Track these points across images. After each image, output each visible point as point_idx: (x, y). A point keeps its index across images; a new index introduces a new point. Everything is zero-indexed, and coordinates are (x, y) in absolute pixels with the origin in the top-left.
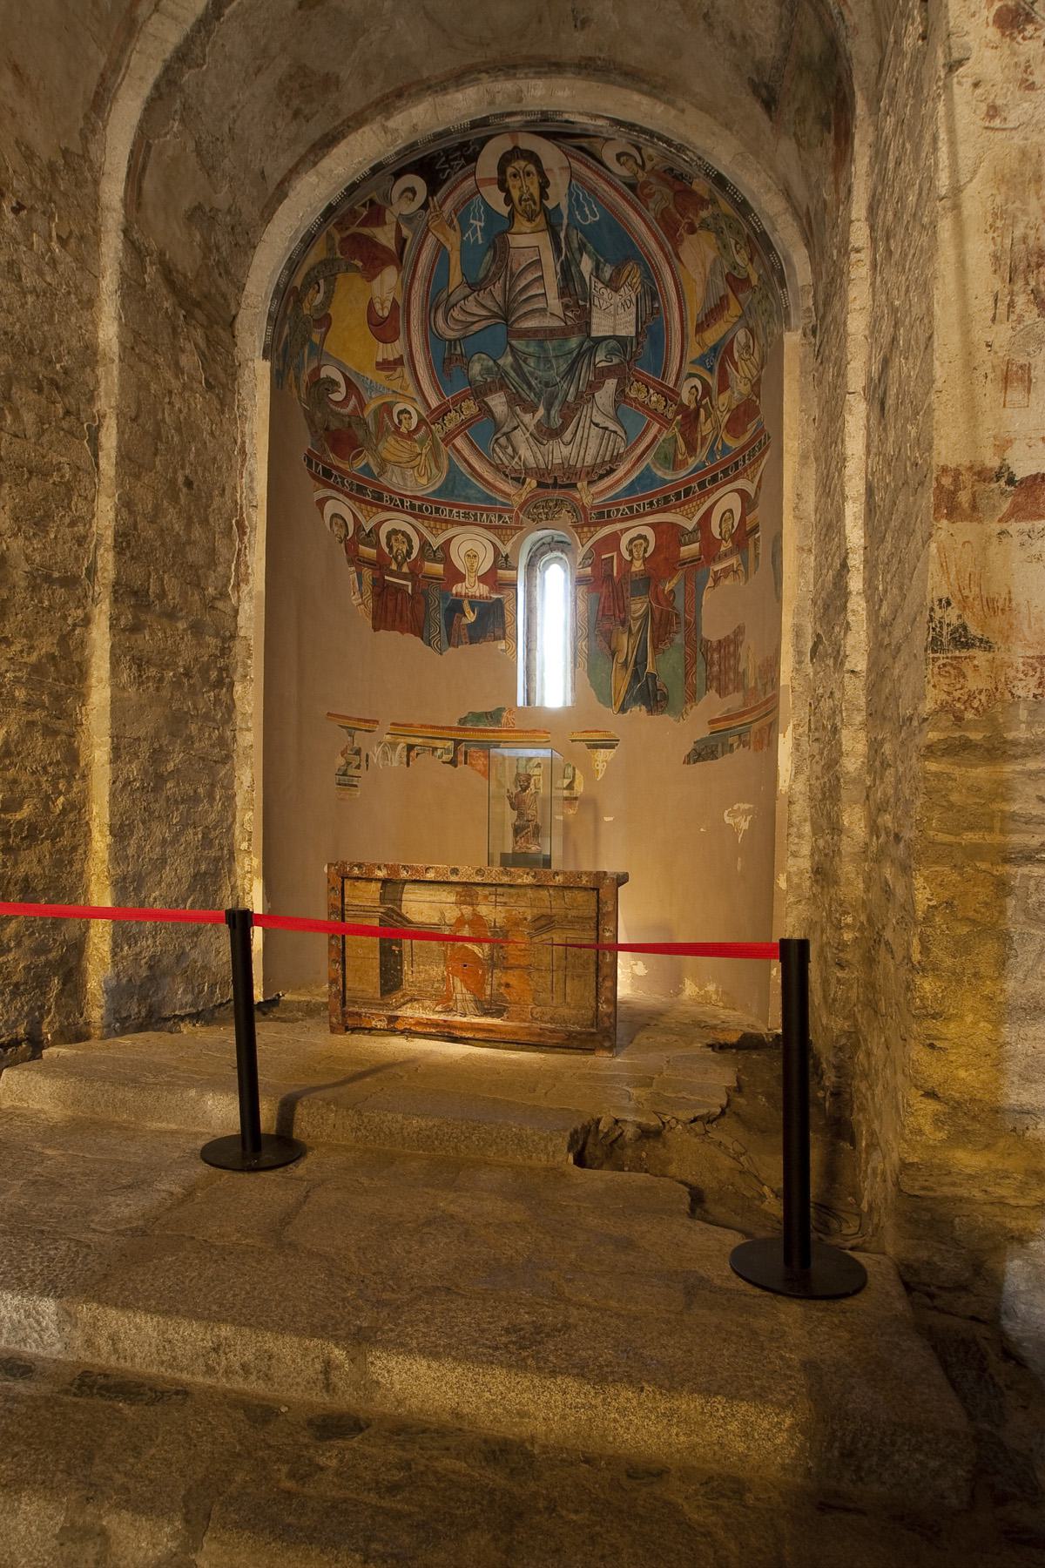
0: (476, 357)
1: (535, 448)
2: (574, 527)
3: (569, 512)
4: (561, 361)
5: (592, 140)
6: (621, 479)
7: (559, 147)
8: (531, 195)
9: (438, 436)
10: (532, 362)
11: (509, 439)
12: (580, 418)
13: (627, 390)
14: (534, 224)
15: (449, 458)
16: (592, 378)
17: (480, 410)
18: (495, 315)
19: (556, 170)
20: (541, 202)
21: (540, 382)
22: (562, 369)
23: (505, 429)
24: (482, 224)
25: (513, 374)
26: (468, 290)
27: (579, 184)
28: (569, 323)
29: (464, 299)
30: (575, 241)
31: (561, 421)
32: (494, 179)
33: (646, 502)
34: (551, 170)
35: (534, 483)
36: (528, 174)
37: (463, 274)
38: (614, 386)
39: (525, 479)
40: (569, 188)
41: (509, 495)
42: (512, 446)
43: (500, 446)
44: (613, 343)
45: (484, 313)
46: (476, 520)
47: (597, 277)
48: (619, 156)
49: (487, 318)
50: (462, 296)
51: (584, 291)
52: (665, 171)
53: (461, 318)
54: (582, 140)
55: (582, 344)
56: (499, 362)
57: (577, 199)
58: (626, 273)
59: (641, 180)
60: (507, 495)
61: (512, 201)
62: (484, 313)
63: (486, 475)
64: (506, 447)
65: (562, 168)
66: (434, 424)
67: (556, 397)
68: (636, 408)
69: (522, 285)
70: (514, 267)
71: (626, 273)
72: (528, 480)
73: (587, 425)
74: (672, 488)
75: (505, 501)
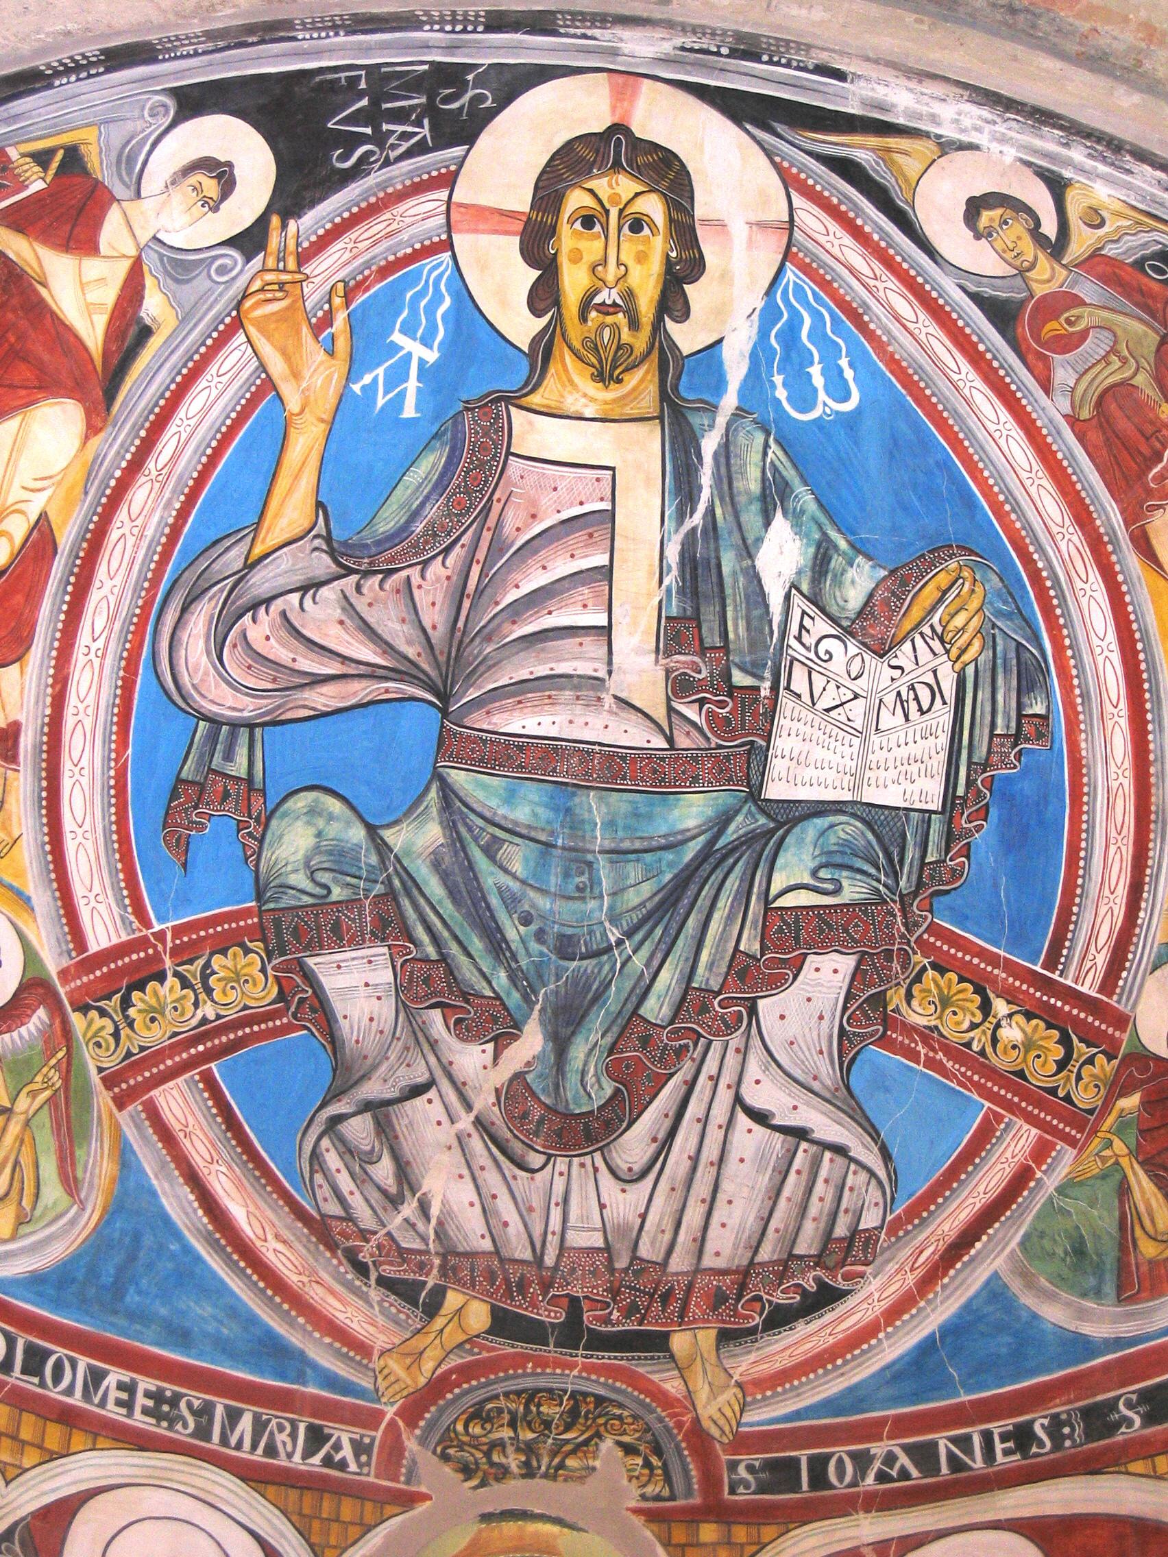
0: (302, 802)
1: (492, 1179)
2: (652, 1516)
3: (629, 1450)
4: (633, 871)
5: (893, 142)
6: (868, 1332)
7: (769, 154)
8: (629, 295)
9: (92, 1062)
10: (518, 857)
11: (384, 1129)
12: (691, 1085)
13: (896, 998)
14: (615, 392)
15: (124, 1156)
16: (751, 944)
17: (281, 996)
18: (405, 671)
19: (739, 230)
20: (658, 324)
21: (540, 936)
22: (632, 898)
23: (373, 1089)
24: (432, 356)
25: (434, 887)
26: (323, 564)
27: (809, 287)
28: (682, 741)
29: (304, 589)
30: (754, 473)
31: (609, 1088)
32: (512, 215)
33: (996, 1427)
34: (721, 225)
35: (479, 1316)
36: (636, 226)
37: (319, 505)
38: (841, 982)
39: (438, 1295)
40: (770, 292)
41: (363, 1348)
42: (396, 1157)
43: (347, 1150)
44: (848, 829)
45: (367, 653)
46: (203, 1432)
47: (814, 600)
48: (975, 207)
49: (372, 673)
50: (298, 579)
51: (757, 640)
52: (1139, 264)
53: (280, 652)
54: (858, 139)
55: (723, 820)
56: (388, 835)
57: (790, 336)
58: (930, 594)
59: (1040, 290)
60: (359, 1348)
61: (557, 303)
62: (367, 653)
63: (274, 1253)
64: (370, 1158)
65: (762, 225)
66: (84, 1009)
67: (599, 997)
68: (931, 1064)
69: (527, 587)
70: (511, 520)
71: (930, 594)
72: (453, 1299)
73: (720, 1113)
74: (1127, 1370)
75: (342, 1370)
